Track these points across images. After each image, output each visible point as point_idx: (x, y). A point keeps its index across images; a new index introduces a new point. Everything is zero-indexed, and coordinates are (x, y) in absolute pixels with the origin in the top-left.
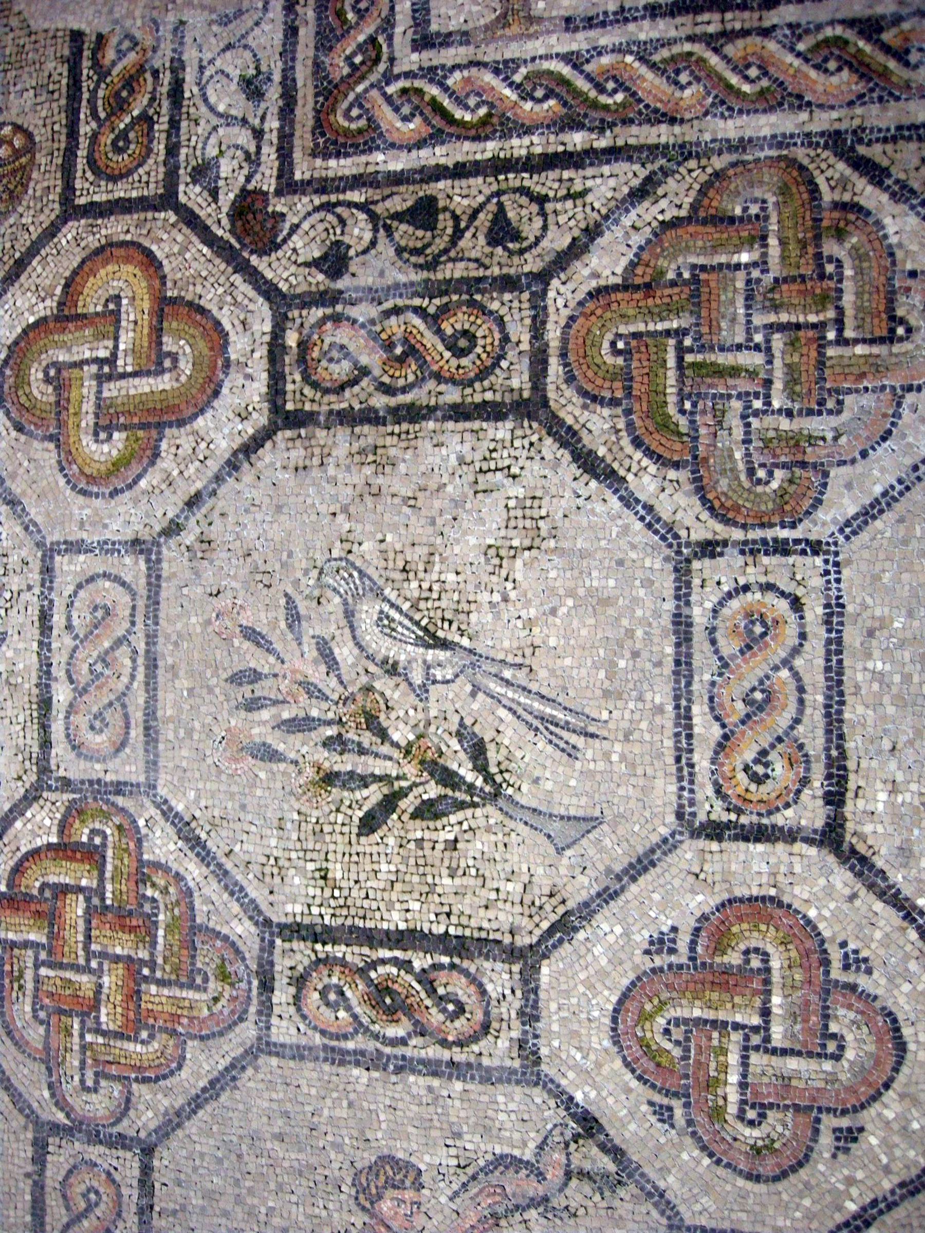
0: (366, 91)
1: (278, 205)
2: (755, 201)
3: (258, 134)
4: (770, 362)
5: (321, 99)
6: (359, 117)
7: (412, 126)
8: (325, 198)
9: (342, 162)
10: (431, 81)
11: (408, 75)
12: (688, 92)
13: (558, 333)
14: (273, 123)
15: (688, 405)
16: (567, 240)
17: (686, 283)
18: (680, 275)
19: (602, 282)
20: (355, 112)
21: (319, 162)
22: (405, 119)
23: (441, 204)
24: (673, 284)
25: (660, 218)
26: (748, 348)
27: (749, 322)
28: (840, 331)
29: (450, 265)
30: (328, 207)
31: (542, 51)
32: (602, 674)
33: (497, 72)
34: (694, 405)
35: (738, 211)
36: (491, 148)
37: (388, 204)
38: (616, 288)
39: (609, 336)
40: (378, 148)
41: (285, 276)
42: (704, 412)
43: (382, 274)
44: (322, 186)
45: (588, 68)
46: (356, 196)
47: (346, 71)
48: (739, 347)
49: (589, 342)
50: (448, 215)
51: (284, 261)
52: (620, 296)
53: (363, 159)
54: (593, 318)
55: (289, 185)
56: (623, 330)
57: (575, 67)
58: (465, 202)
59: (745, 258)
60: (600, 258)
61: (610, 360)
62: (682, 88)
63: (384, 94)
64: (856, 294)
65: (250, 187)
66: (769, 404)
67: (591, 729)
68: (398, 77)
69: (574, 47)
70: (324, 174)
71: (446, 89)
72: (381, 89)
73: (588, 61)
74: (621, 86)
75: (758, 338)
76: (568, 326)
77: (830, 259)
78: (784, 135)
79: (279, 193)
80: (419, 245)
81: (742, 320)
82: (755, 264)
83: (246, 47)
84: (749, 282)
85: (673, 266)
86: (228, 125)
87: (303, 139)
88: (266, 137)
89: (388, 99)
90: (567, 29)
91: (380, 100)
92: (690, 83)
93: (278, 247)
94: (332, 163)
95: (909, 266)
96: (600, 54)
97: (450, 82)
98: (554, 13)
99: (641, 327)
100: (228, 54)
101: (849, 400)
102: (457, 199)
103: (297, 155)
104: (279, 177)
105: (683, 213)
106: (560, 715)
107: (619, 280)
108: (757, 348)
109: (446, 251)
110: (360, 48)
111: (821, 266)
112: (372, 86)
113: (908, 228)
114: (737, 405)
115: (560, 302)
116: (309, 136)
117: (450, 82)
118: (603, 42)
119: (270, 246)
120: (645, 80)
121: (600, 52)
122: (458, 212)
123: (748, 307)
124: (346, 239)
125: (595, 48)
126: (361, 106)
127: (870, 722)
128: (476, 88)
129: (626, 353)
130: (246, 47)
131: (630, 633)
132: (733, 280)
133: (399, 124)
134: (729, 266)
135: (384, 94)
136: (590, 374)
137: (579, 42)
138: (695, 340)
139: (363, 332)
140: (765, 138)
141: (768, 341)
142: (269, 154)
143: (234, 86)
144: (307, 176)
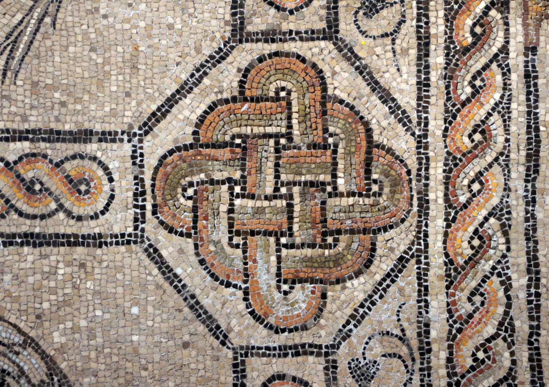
4: (266, 198)
12: (466, 140)
13: (294, 50)
15: (238, 141)
16: (360, 54)
17: (325, 139)
18: (331, 135)
19: (328, 81)
24: (326, 130)
25: (374, 121)
26: (276, 183)
27: (295, 184)
28: (286, 246)
32: (49, 81)
34: (238, 146)
35: (375, 176)
38: (325, 89)
39: (289, 86)
42: (232, 152)
45: (494, 66)
48: (277, 177)
49: (285, 72)
52: (319, 93)
54: (303, 74)
56: (294, 95)
57: (496, 56)
59: (340, 181)
60: (347, 79)
61: (273, 87)
62: (470, 136)
64: (312, 257)
67: (9, 74)
73: (499, 66)
74: (476, 92)
75: (283, 190)
76: (298, 57)
78: (428, 208)
81: (297, 178)
82: (335, 188)
84: (323, 184)
85: (338, 131)
92: (473, 141)
96: (504, 74)
99: (295, 109)
105: (376, 138)
106: (18, 54)
107: (330, 92)
108: (277, 189)
115: (316, 50)
118: (514, 76)
123: (305, 183)
125: (509, 71)
127: (22, 265)
129: (277, 99)
131: (78, 100)
132: (324, 173)
134: (335, 170)
136: (263, 73)
138: (284, 146)
140: (427, 195)
141: (281, 197)
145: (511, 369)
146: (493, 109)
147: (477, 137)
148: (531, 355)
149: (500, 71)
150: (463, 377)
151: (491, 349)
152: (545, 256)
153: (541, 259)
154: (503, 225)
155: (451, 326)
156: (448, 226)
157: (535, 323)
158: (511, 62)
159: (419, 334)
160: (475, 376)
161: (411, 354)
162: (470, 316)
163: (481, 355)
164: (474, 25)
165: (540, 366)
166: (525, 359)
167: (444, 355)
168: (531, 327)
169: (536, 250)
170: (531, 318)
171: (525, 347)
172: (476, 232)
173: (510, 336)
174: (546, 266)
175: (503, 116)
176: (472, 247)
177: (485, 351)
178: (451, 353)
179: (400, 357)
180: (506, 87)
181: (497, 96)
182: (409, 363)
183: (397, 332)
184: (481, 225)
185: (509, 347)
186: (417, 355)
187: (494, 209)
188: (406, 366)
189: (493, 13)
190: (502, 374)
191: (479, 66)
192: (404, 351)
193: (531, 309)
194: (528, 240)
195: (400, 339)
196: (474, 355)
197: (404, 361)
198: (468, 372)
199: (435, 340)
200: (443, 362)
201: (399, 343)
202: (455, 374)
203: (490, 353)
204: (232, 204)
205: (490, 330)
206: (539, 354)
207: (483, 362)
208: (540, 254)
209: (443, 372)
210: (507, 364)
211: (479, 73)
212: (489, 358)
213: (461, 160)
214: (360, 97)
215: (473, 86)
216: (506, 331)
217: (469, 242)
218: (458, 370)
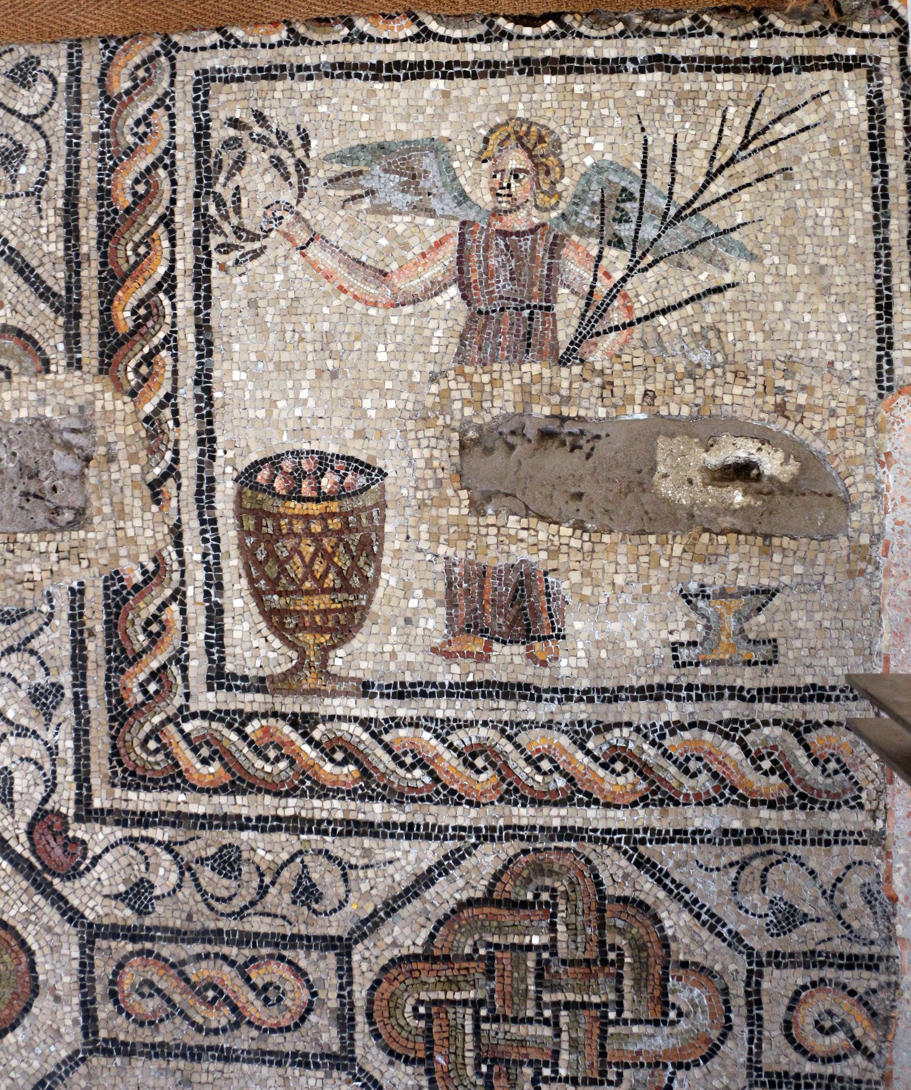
0: (163, 723)
1: (78, 831)
2: (546, 889)
3: (52, 751)
4: (558, 1035)
5: (116, 724)
6: (157, 751)
7: (212, 770)
8: (127, 832)
9: (143, 795)
10: (230, 726)
11: (204, 715)
12: (483, 777)
13: (364, 993)
14: (67, 744)
15: (484, 1068)
16: (370, 909)
17: (481, 958)
18: (476, 951)
19: (404, 952)
20: (152, 745)
21: (118, 792)
22: (205, 762)
23: (245, 855)
24: (469, 958)
25: (457, 896)
26: (539, 1022)
27: (539, 999)
28: (620, 1012)
29: (257, 919)
30: (132, 841)
31: (340, 712)
33: (294, 725)
34: (490, 1068)
35: (530, 896)
36: (291, 807)
37: (192, 846)
38: (416, 957)
39: (411, 1002)
40: (178, 787)
41: (91, 904)
42: (498, 1076)
43: (189, 918)
44: (121, 818)
45: (387, 738)
46: (160, 834)
47: (140, 698)
48: (530, 1021)
49: (394, 1005)
50: (253, 868)
51: (88, 890)
52: (420, 966)
53: (164, 796)
54: (396, 983)
55: (89, 812)
56: (423, 996)
57: (373, 735)
58: (269, 857)
59: (536, 940)
60: (402, 928)
61: (414, 1023)
62: (478, 772)
63: (181, 731)
64: (634, 980)
65: (48, 807)
66: (555, 1071)
68: (194, 716)
69: (372, 714)
70: (124, 806)
71: (245, 737)
72: (177, 725)
73: (387, 731)
74: (420, 763)
75: (547, 1013)
76: (373, 988)
77: (613, 948)
78: (572, 828)
79: (78, 818)
80: (226, 894)
81: (532, 995)
82: (545, 947)
83: (33, 652)
84: (539, 962)
85: (470, 942)
86: (19, 735)
87: (99, 765)
88: (61, 755)
89: (186, 737)
90: (365, 695)
91: (178, 737)
92: (485, 768)
93: (81, 875)
94: (132, 795)
95: (681, 957)
96: (398, 726)
97: (249, 729)
98: (352, 674)
99: (442, 996)
100: (14, 656)
101: (627, 1073)
102: (261, 852)
103: (95, 781)
104: (78, 802)
105: (479, 895)
107: (419, 951)
108: (546, 1022)
109: (253, 903)
110: (153, 675)
111: (604, 953)
112: (169, 720)
113: (682, 923)
114: (528, 1071)
115: (365, 966)
116: (105, 762)
117: (249, 729)
118: (401, 713)
119: (73, 873)
120: (443, 760)
121: (398, 723)
122: (263, 867)
123: (538, 984)
124: (152, 878)
125: (393, 719)
126: (158, 740)
128: (275, 739)
129: (428, 1017)
130: (33, 652)
132: (525, 960)
133: (198, 765)
134: (520, 947)
135: (181, 731)
136: (394, 1034)
137: (378, 709)
138: (490, 1011)
139: (173, 972)
141: (556, 1017)
142: (66, 776)
143: (22, 694)
144: (107, 805)
145: (786, 727)
146: (444, 741)
147: (480, 762)
148: (768, 700)
149: (393, 731)
150: (794, 789)
151: (758, 751)
152: (639, 677)
153: (643, 682)
154: (597, 731)
155: (727, 801)
156: (596, 802)
157: (727, 693)
158: (382, 715)
159: (737, 843)
160: (793, 773)
161: (762, 854)
162: (715, 775)
163: (766, 764)
164: (332, 760)
165: (783, 689)
166: (773, 707)
167: (765, 813)
168: (731, 697)
169: (632, 689)
170: (720, 697)
171: (757, 706)
172: (604, 766)
173: (742, 725)
174: (651, 676)
175: (453, 728)
176: (625, 771)
177: (762, 758)
178: (763, 802)
179: (766, 870)
180: (414, 724)
181: (427, 735)
182: (774, 858)
183: (733, 872)
184: (596, 759)
185: (757, 727)
186: (764, 848)
187: (575, 742)
188: (778, 862)
189: (317, 734)
190: (791, 739)
191: (386, 758)
192: (759, 865)
193: (707, 696)
194: (617, 699)
195: (742, 868)
196: (766, 773)
197: (772, 865)
198: (788, 781)
199: (745, 822)
200: (774, 814)
201: (747, 870)
202: (790, 798)
203: (764, 751)
204: (566, 1080)
205: (734, 750)
206: (767, 690)
207: (775, 762)
208: (636, 684)
209: (787, 814)
210: (778, 731)
211: (395, 758)
212: (770, 755)
213: (510, 784)
214: (425, 912)
215: (413, 766)
216: (736, 730)
217: (618, 775)
218: (785, 795)
